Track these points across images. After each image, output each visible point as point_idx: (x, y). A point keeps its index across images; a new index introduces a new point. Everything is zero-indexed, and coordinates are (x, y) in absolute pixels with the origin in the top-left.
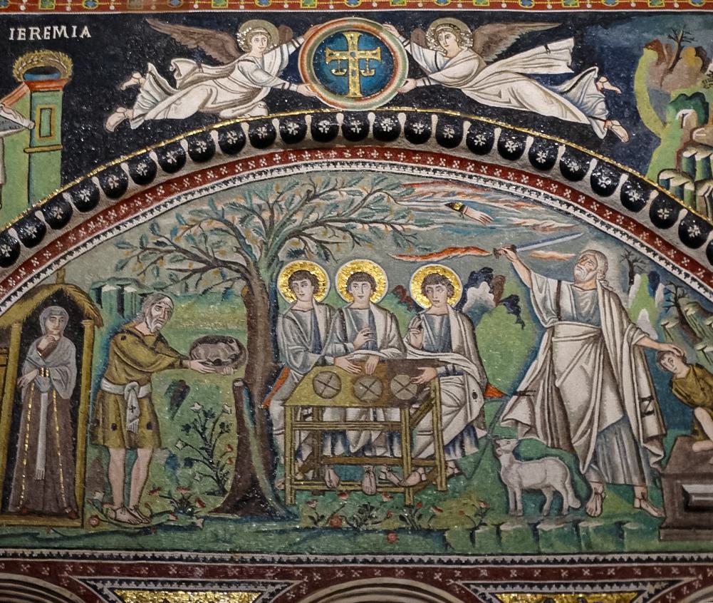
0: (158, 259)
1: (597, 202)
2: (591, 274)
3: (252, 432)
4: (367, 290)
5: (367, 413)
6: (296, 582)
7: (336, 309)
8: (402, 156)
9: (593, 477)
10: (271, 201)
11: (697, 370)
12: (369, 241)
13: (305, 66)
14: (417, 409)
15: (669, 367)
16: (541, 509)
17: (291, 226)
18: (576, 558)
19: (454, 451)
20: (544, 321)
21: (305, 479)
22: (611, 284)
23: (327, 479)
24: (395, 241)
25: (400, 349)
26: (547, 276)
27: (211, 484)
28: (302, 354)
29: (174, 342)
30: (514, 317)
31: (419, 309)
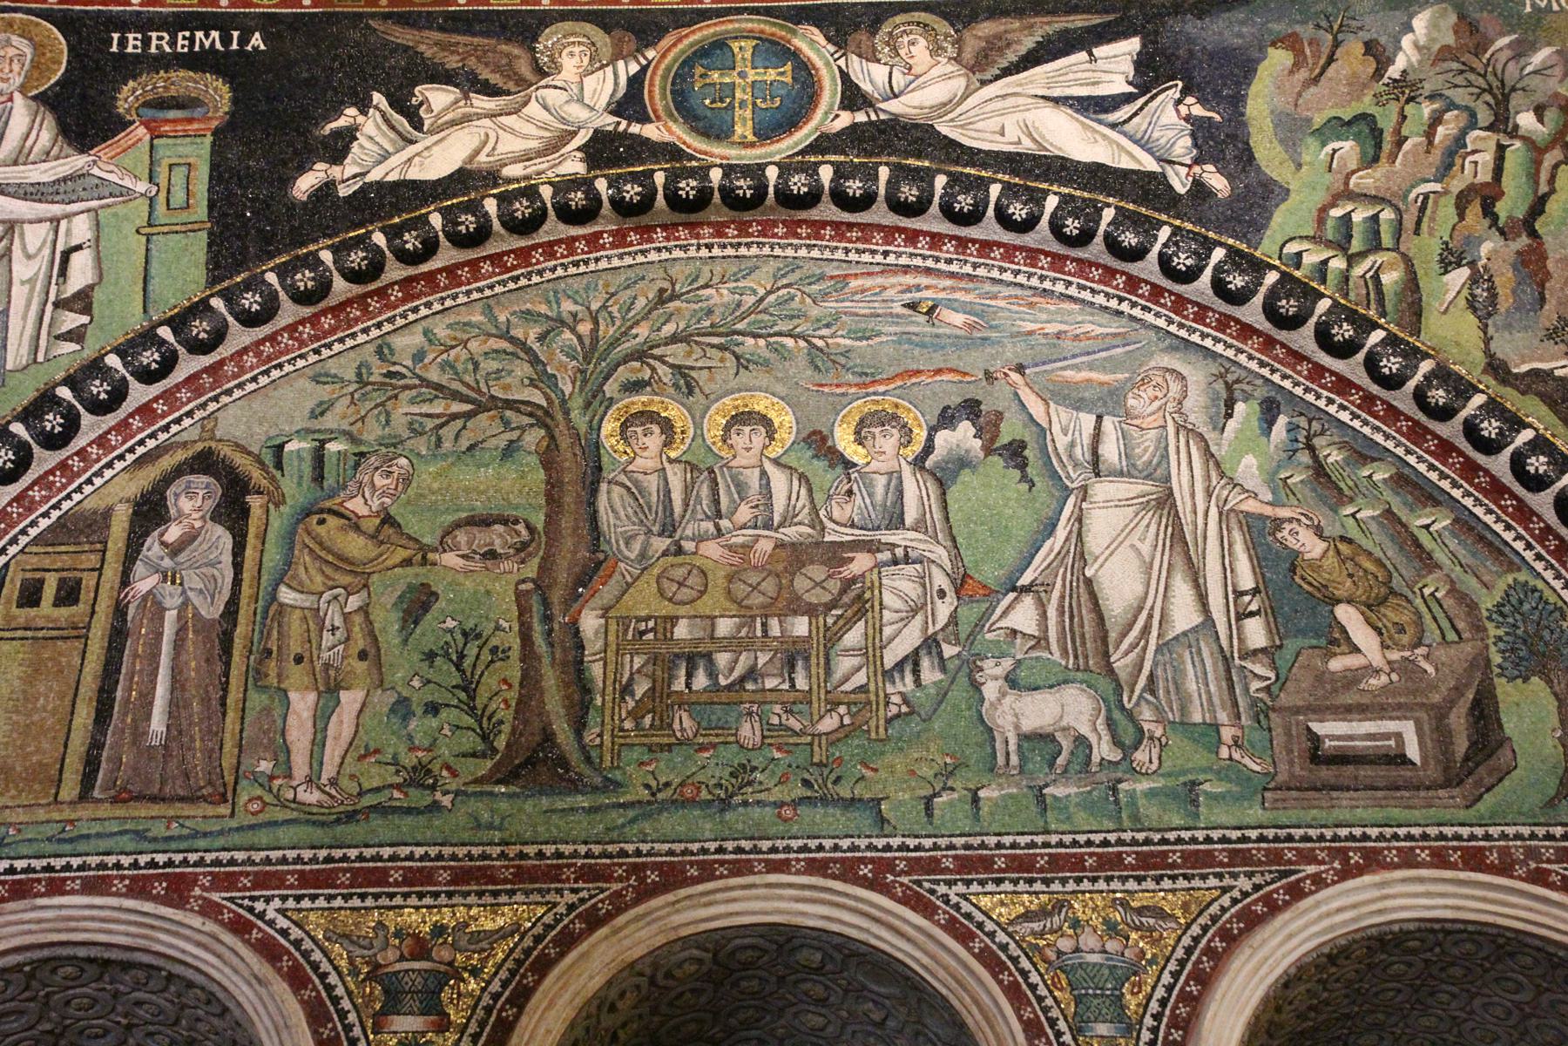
0: (389, 399)
1: (1171, 293)
2: (1157, 404)
3: (546, 661)
4: (759, 439)
5: (752, 627)
6: (616, 886)
7: (701, 470)
8: (828, 232)
9: (1146, 714)
10: (595, 306)
11: (1343, 547)
12: (766, 363)
13: (656, 94)
14: (839, 617)
15: (1291, 542)
16: (1052, 764)
17: (627, 345)
18: (1112, 837)
19: (903, 678)
20: (1069, 477)
21: (638, 727)
22: (1192, 418)
23: (676, 726)
24: (812, 362)
25: (813, 527)
26: (1078, 409)
27: (470, 741)
28: (641, 538)
29: (413, 524)
30: (1017, 474)
31: (848, 465)
